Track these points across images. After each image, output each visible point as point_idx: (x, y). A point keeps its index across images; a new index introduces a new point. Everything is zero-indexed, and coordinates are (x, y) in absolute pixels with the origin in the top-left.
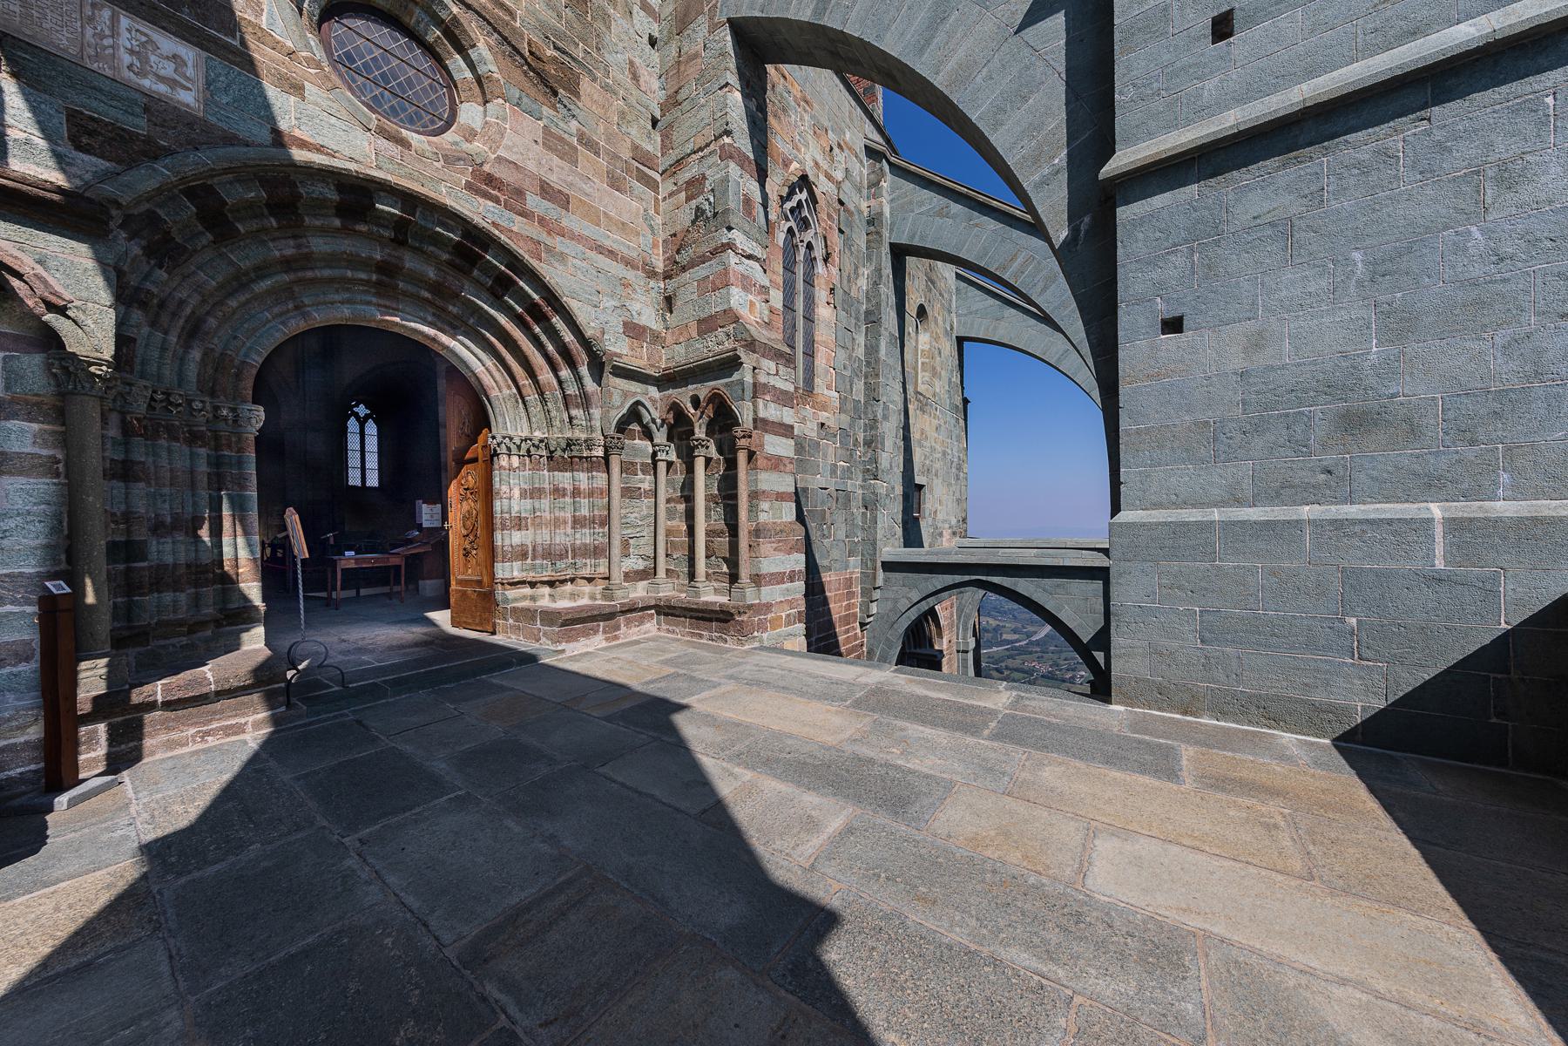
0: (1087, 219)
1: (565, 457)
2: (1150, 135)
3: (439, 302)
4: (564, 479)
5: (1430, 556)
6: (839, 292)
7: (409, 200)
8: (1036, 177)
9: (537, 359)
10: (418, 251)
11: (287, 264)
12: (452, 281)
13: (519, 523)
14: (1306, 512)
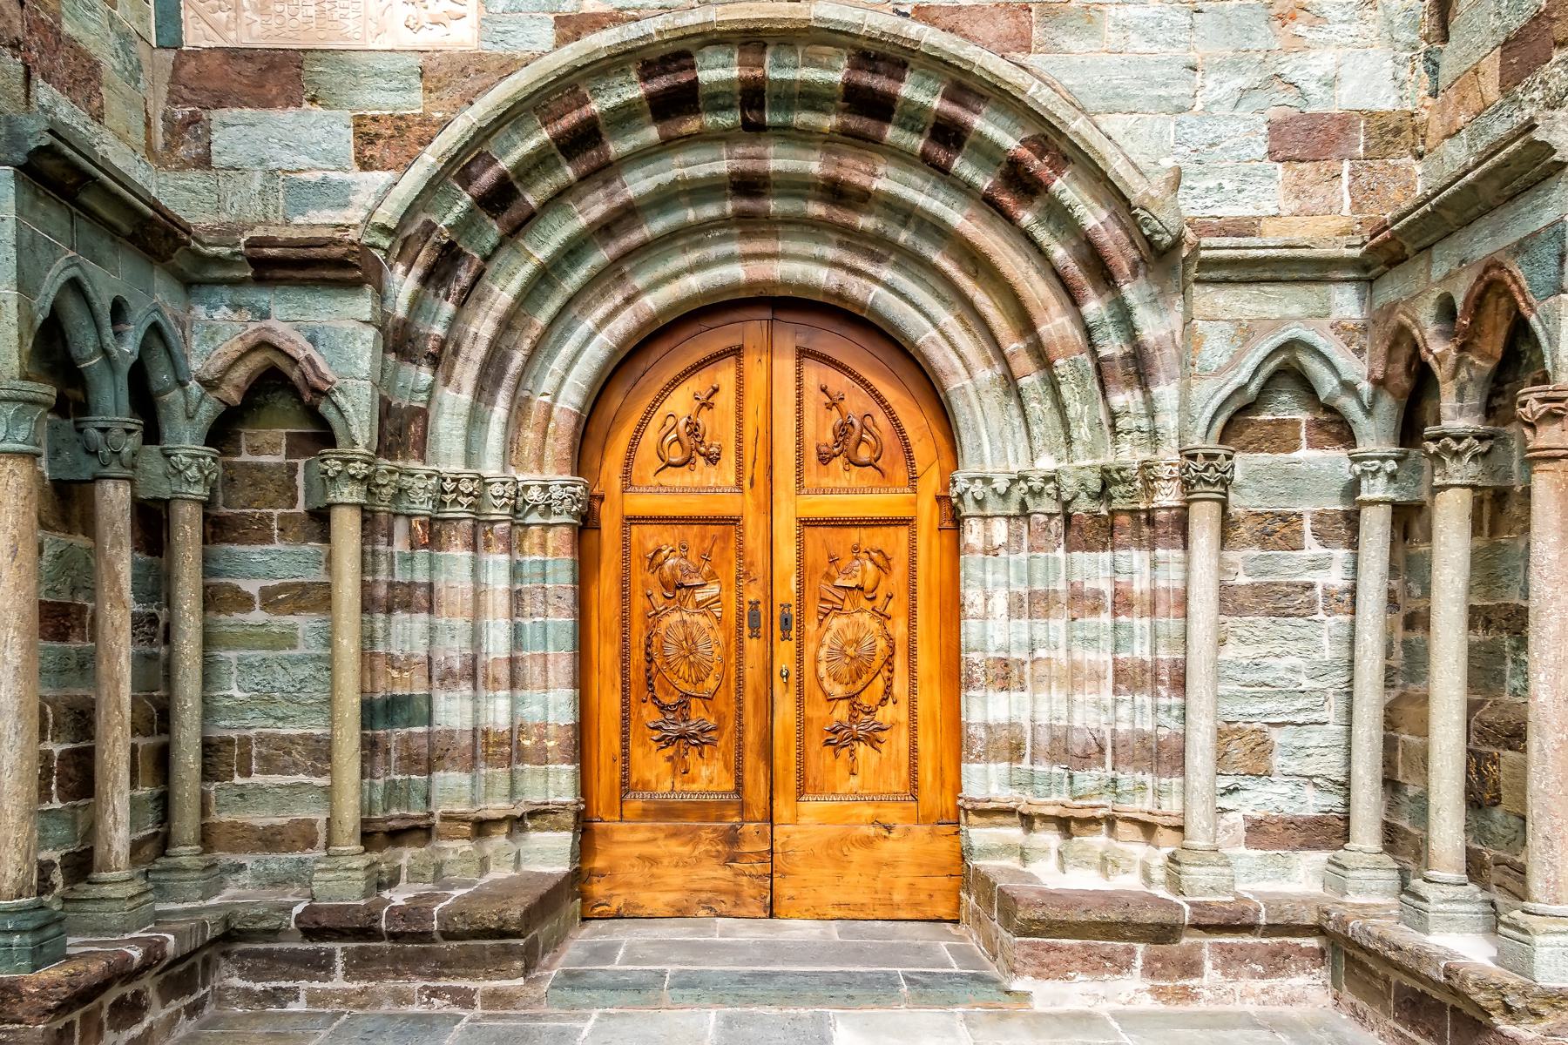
1: (1104, 516)
3: (841, 216)
4: (1094, 569)
7: (751, 40)
9: (1035, 288)
10: (787, 134)
11: (605, 229)
12: (854, 171)
13: (1005, 675)
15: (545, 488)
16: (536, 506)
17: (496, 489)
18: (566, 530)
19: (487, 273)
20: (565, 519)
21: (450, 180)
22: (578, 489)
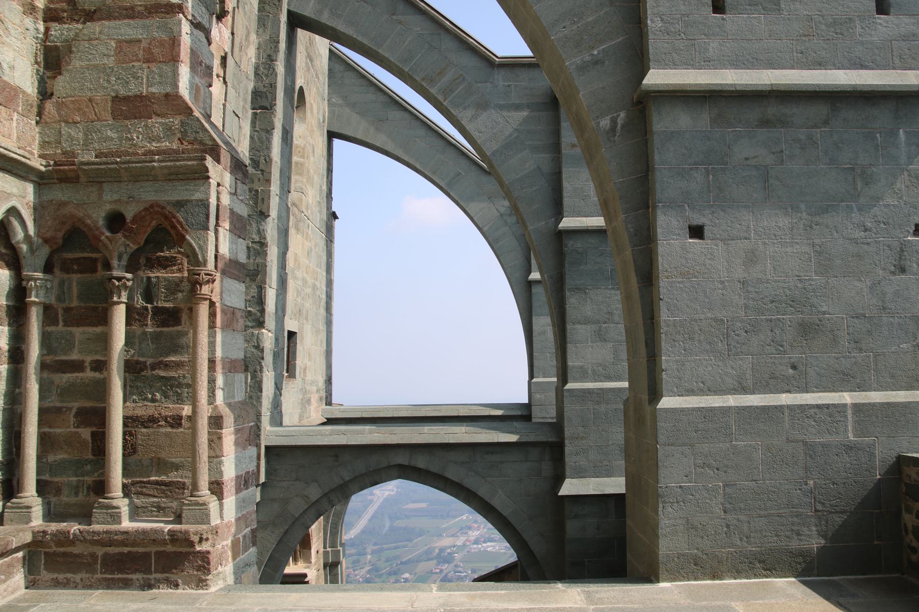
0: (623, 115)
2: (675, 65)
5: (846, 431)
6: (230, 62)
8: (578, 60)
14: (785, 399)
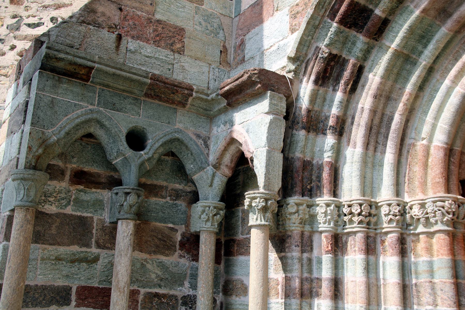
15: (423, 206)
16: (419, 219)
17: (384, 210)
18: (442, 236)
19: (366, 69)
20: (440, 227)
21: (326, 18)
22: (447, 204)
